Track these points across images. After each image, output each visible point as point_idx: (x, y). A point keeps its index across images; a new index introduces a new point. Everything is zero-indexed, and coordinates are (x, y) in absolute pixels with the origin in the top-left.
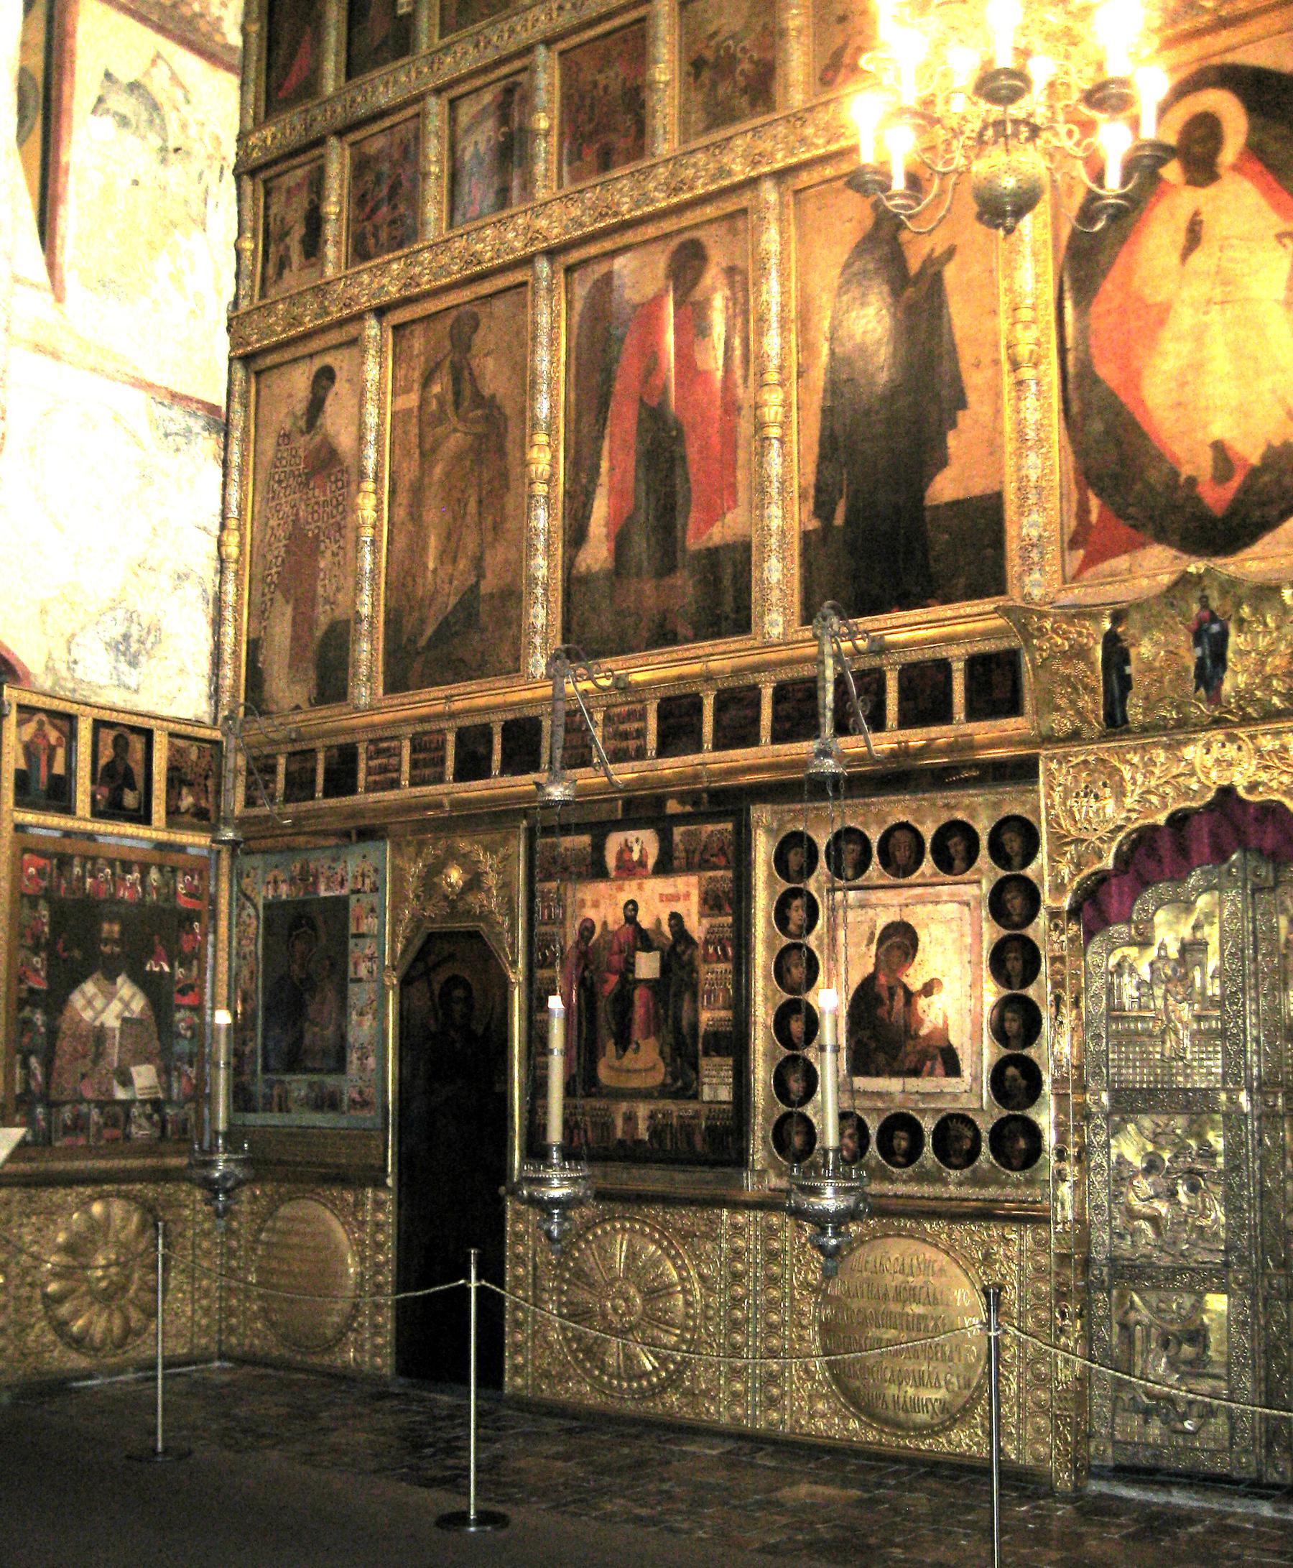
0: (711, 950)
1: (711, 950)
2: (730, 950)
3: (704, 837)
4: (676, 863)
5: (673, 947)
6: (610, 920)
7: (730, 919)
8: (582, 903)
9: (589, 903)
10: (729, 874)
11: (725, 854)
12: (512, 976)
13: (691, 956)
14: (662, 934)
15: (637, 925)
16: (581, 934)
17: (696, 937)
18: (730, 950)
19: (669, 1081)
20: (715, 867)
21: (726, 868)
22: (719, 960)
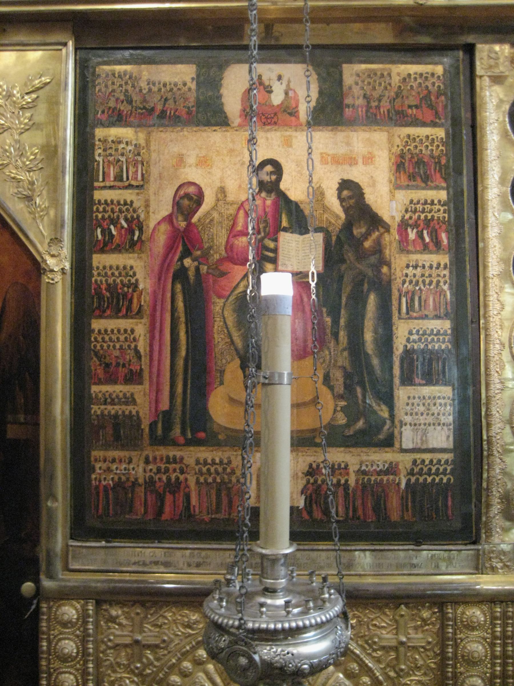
0: (412, 235)
1: (412, 235)
2: (444, 236)
3: (396, 80)
4: (348, 112)
5: (348, 226)
6: (231, 186)
7: (443, 195)
8: (181, 160)
9: (191, 160)
10: (440, 133)
11: (431, 107)
12: (51, 262)
13: (378, 243)
14: (326, 209)
15: (282, 196)
16: (177, 204)
17: (386, 218)
18: (444, 236)
19: (342, 420)
20: (416, 123)
21: (434, 125)
22: (425, 248)
